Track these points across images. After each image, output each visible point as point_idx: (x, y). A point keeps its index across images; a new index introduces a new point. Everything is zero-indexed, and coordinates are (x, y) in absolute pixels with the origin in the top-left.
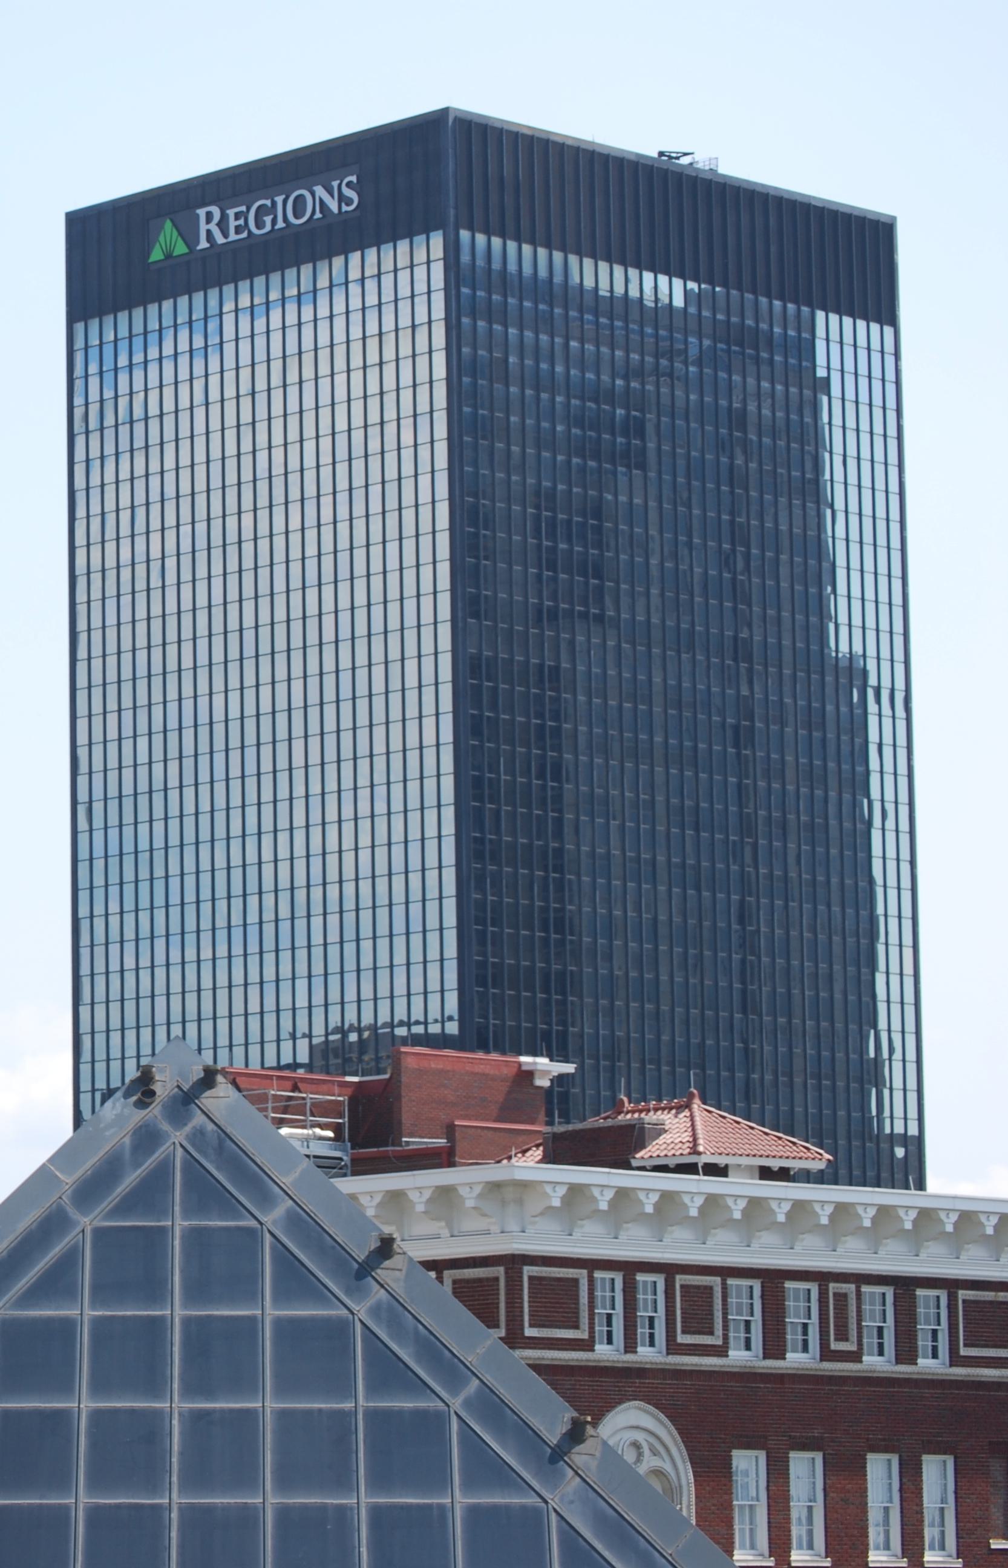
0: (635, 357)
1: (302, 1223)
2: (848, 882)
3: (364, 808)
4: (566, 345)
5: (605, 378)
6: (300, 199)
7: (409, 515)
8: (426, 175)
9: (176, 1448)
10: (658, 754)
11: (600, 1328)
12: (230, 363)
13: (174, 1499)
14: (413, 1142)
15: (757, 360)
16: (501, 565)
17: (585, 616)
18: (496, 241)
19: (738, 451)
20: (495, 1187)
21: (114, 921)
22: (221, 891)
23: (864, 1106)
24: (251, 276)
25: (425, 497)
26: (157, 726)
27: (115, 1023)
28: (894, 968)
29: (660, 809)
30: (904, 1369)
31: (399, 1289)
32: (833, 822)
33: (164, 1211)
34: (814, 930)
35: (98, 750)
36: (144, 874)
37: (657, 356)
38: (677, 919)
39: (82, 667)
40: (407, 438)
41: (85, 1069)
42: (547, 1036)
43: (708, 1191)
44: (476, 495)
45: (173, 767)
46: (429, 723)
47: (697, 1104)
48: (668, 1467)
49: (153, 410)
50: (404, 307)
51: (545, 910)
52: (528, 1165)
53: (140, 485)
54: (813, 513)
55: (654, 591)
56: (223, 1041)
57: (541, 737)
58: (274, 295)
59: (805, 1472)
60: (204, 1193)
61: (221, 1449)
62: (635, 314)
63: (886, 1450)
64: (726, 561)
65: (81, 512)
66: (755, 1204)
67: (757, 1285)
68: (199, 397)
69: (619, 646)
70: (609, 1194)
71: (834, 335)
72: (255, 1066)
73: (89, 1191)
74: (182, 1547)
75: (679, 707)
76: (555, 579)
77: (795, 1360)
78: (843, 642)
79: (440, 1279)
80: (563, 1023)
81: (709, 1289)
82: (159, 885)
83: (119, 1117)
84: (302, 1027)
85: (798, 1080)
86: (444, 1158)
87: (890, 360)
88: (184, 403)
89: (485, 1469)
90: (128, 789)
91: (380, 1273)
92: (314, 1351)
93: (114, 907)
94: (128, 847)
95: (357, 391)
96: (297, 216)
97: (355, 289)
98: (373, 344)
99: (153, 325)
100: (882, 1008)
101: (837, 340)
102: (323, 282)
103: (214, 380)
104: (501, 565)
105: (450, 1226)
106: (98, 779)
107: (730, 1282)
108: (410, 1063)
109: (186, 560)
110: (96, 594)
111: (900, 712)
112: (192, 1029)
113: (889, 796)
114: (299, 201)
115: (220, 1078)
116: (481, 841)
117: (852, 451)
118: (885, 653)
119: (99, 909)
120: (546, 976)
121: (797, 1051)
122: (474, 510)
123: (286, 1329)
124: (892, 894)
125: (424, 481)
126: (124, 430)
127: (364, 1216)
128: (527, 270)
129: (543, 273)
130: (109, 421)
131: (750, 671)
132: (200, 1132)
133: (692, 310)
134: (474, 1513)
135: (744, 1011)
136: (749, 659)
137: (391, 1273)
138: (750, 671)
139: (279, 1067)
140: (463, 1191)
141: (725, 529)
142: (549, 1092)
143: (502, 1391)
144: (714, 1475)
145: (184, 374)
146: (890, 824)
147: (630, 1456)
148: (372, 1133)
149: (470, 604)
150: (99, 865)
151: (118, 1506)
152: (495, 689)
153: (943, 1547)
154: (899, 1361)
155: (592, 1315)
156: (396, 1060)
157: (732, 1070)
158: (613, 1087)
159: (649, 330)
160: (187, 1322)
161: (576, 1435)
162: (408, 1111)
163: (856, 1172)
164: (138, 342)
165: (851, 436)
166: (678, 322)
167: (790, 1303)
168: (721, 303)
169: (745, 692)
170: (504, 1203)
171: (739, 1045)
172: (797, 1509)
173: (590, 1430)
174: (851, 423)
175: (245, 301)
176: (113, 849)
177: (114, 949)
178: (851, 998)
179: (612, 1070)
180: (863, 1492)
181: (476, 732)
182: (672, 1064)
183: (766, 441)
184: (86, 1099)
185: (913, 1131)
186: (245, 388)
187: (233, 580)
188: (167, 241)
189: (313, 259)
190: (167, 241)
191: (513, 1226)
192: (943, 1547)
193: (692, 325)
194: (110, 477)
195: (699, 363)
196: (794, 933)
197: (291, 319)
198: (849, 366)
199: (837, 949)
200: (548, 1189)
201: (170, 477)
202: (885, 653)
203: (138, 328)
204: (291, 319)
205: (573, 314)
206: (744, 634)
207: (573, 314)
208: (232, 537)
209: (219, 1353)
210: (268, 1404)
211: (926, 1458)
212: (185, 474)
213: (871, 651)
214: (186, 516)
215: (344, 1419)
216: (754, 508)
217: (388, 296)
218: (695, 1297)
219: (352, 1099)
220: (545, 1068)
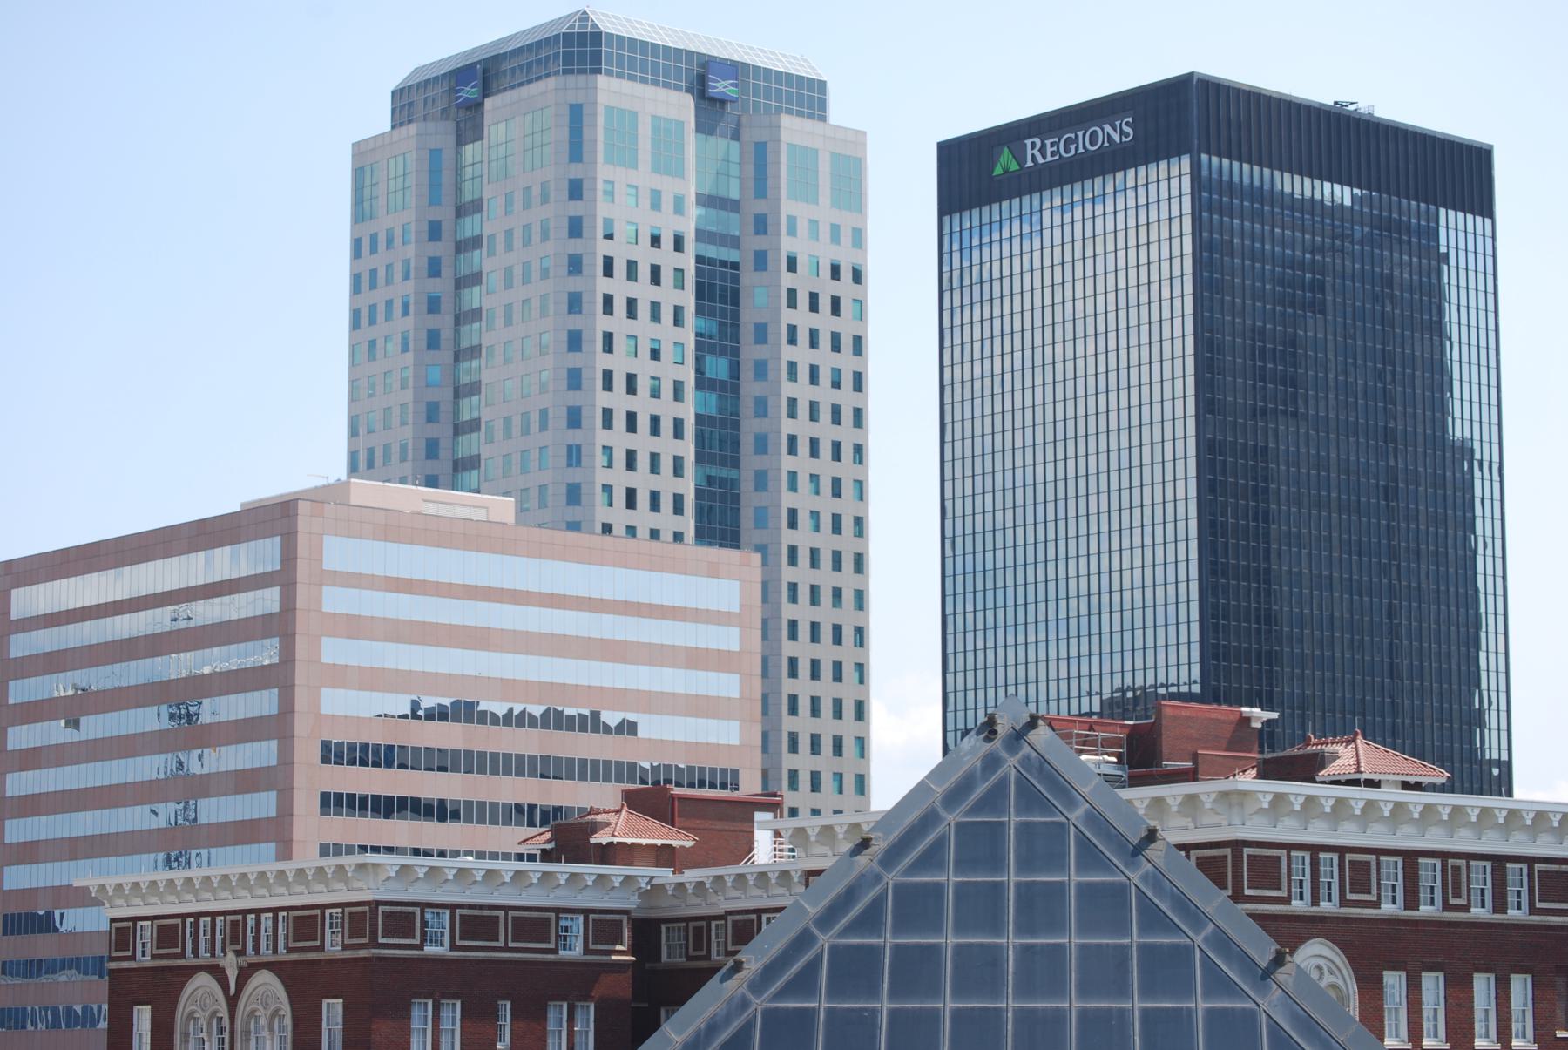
0: (1318, 239)
1: (1095, 819)
2: (1461, 590)
3: (1137, 541)
4: (1272, 231)
5: (1298, 253)
6: (1094, 134)
7: (1167, 345)
8: (1180, 117)
9: (1011, 970)
10: (1334, 505)
11: (1295, 890)
12: (1047, 243)
13: (1010, 1004)
14: (1170, 765)
15: (1400, 241)
16: (1229, 379)
17: (1285, 412)
18: (1226, 162)
19: (1387, 302)
20: (1225, 795)
21: (970, 617)
22: (1041, 597)
23: (1472, 741)
24: (1061, 185)
25: (1178, 333)
26: (999, 486)
27: (970, 685)
28: (1492, 648)
29: (1335, 542)
30: (1499, 917)
31: (1160, 863)
32: (1451, 551)
33: (1003, 811)
34: (1438, 622)
35: (959, 502)
36: (990, 585)
37: (1333, 239)
38: (1346, 616)
39: (948, 447)
40: (1166, 294)
41: (950, 716)
42: (1259, 694)
43: (1366, 797)
44: (1211, 331)
45: (1009, 514)
46: (1180, 484)
47: (1360, 739)
48: (1340, 983)
49: (996, 275)
50: (1164, 206)
51: (1258, 609)
52: (1247, 780)
53: (987, 324)
54: (1437, 343)
55: (1331, 396)
56: (1042, 697)
57: (1255, 493)
58: (1077, 198)
59: (1433, 986)
60: (1030, 799)
61: (1042, 970)
62: (1318, 210)
63: (1487, 971)
64: (1380, 376)
65: (947, 343)
66: (1399, 806)
67: (1400, 861)
68: (1026, 266)
69: (1307, 434)
70: (1301, 800)
71: (1452, 225)
72: (1064, 713)
73: (953, 797)
74: (1015, 1035)
75: (1348, 473)
76: (1265, 388)
77: (1426, 911)
78: (1458, 430)
79: (1188, 856)
80: (1271, 685)
81: (1368, 863)
82: (1000, 593)
83: (974, 749)
84: (1096, 688)
85: (1427, 723)
86: (1190, 776)
87: (1489, 241)
88: (1017, 269)
89: (1218, 983)
90: (979, 529)
91: (1148, 853)
92: (1105, 905)
93: (970, 608)
94: (979, 567)
95: (1132, 262)
96: (1094, 132)
97: (1131, 194)
98: (1143, 230)
99: (996, 217)
100: (1483, 675)
101: (1453, 227)
102: (1109, 189)
103: (1037, 255)
104: (1229, 379)
105: (1194, 820)
106: (959, 522)
107: (1382, 858)
108: (1168, 712)
109: (1018, 375)
110: (958, 398)
111: (1496, 477)
112: (1022, 688)
113: (1488, 533)
114: (1094, 136)
115: (1040, 722)
116: (1215, 563)
117: (1463, 302)
118: (1486, 438)
119: (960, 609)
120: (1259, 653)
121: (1427, 704)
122: (1211, 341)
123: (1085, 891)
124: (1491, 599)
125: (1177, 322)
126: (976, 288)
127: (1136, 814)
128: (1246, 181)
129: (1257, 183)
130: (967, 282)
131: (1396, 448)
132: (1027, 758)
133: (1357, 207)
134: (1210, 1013)
135: (1392, 677)
136: (1395, 441)
137: (1155, 853)
138: (1396, 448)
139: (1080, 715)
140: (1203, 798)
141: (1379, 354)
142: (1261, 731)
143: (1229, 931)
144: (1371, 988)
145: (1016, 251)
146: (1489, 552)
147: (1315, 975)
148: (1143, 758)
149: (1207, 405)
150: (960, 579)
151: (972, 1009)
152: (1225, 462)
153: (1524, 1036)
154: (1495, 911)
155: (1289, 881)
156: (1159, 710)
157: (1383, 716)
158: (1303, 727)
159: (1328, 221)
160: (1018, 885)
161: (1279, 961)
162: (1166, 745)
163: (1467, 785)
164: (986, 229)
165: (1463, 292)
166: (1347, 216)
167: (1422, 873)
168: (1376, 202)
169: (1392, 463)
170: (1230, 806)
171: (1388, 700)
172: (1427, 1010)
173: (1288, 957)
174: (1463, 283)
175: (1057, 202)
176: (969, 569)
177: (970, 635)
178: (1463, 668)
179: (1303, 716)
180: (1471, 999)
181: (1213, 490)
182: (1343, 712)
183: (1406, 295)
184: (950, 736)
185: (1504, 757)
186: (1057, 260)
187: (1049, 389)
188: (1005, 162)
189: (1103, 174)
190: (1005, 162)
191: (1237, 821)
192: (1524, 1036)
193: (1357, 217)
194: (967, 319)
195: (1362, 243)
196: (1425, 625)
197: (1088, 214)
198: (1462, 245)
199: (1453, 636)
200: (1260, 796)
201: (1007, 320)
202: (1486, 438)
203: (986, 220)
204: (1088, 214)
205: (1277, 210)
206: (1391, 425)
207: (1277, 210)
208: (1049, 360)
209: (1040, 907)
210: (1073, 940)
211: (1513, 976)
212: (1017, 318)
213: (1476, 436)
214: (1017, 346)
215: (1123, 951)
216: (1398, 340)
217: (1153, 198)
218: (1358, 869)
219: (1130, 737)
220: (1258, 715)
